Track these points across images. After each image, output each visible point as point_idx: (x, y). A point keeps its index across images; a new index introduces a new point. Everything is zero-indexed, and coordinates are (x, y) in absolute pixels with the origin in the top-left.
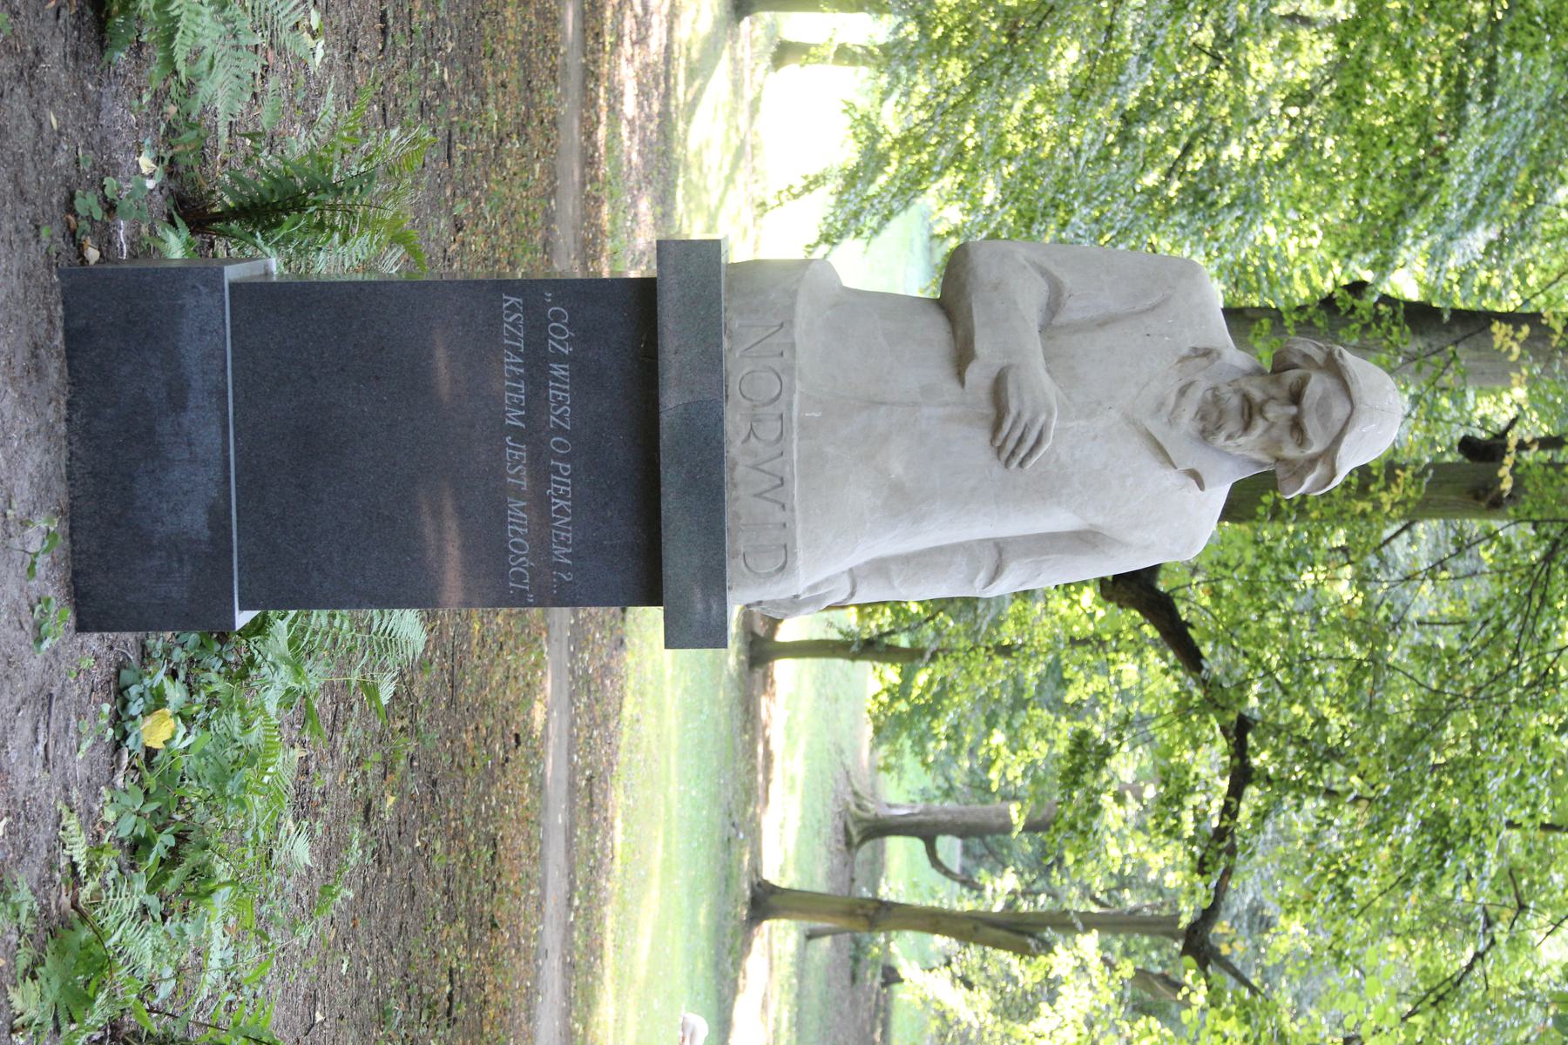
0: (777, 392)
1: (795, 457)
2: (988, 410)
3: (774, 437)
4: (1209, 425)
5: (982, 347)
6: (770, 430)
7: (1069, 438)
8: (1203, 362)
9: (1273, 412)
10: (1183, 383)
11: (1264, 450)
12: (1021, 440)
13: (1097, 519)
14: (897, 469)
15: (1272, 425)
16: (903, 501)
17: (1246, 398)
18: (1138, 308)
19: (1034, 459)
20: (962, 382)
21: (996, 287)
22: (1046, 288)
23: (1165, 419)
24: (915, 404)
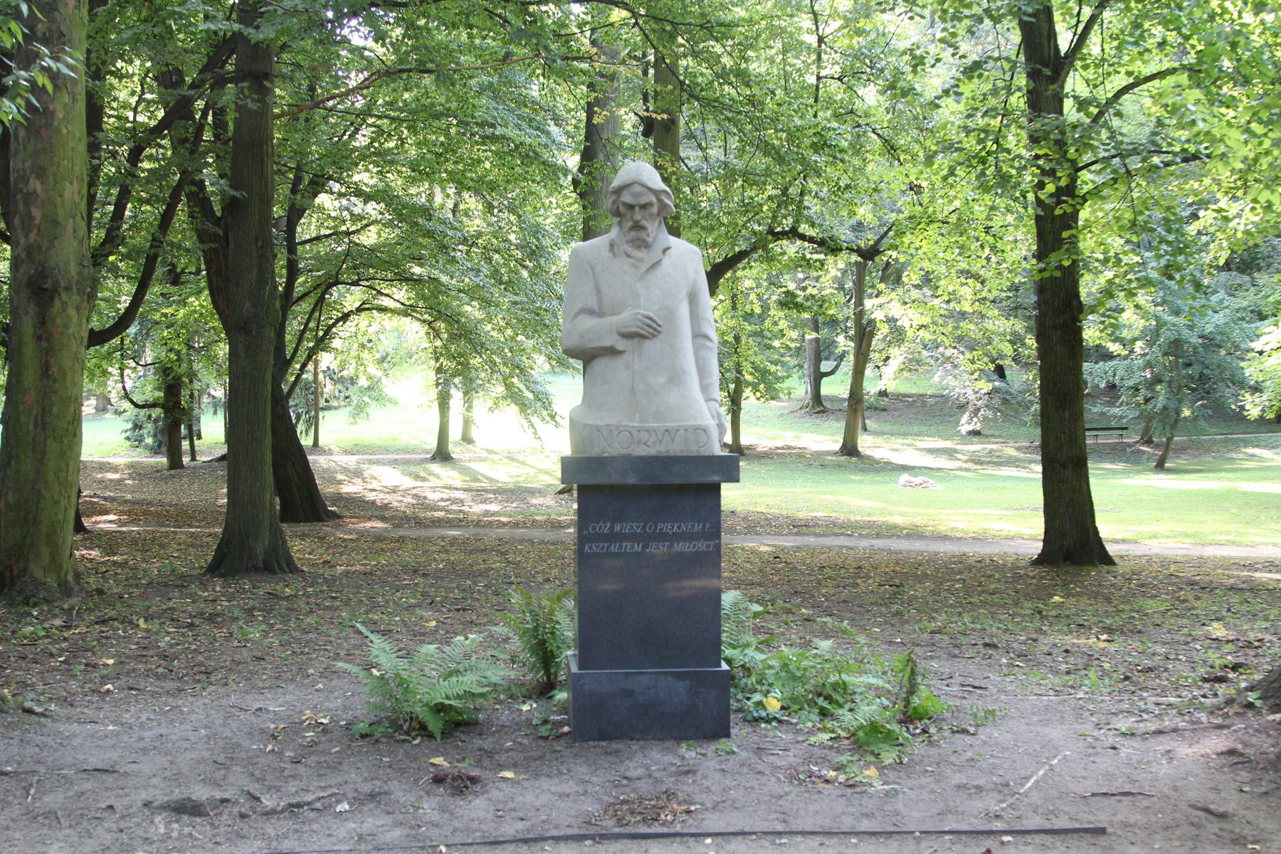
2: (636, 340)
4: (643, 245)
7: (649, 305)
9: (638, 217)
13: (684, 293)
14: (662, 380)
16: (676, 378)
17: (631, 228)
21: (582, 337)
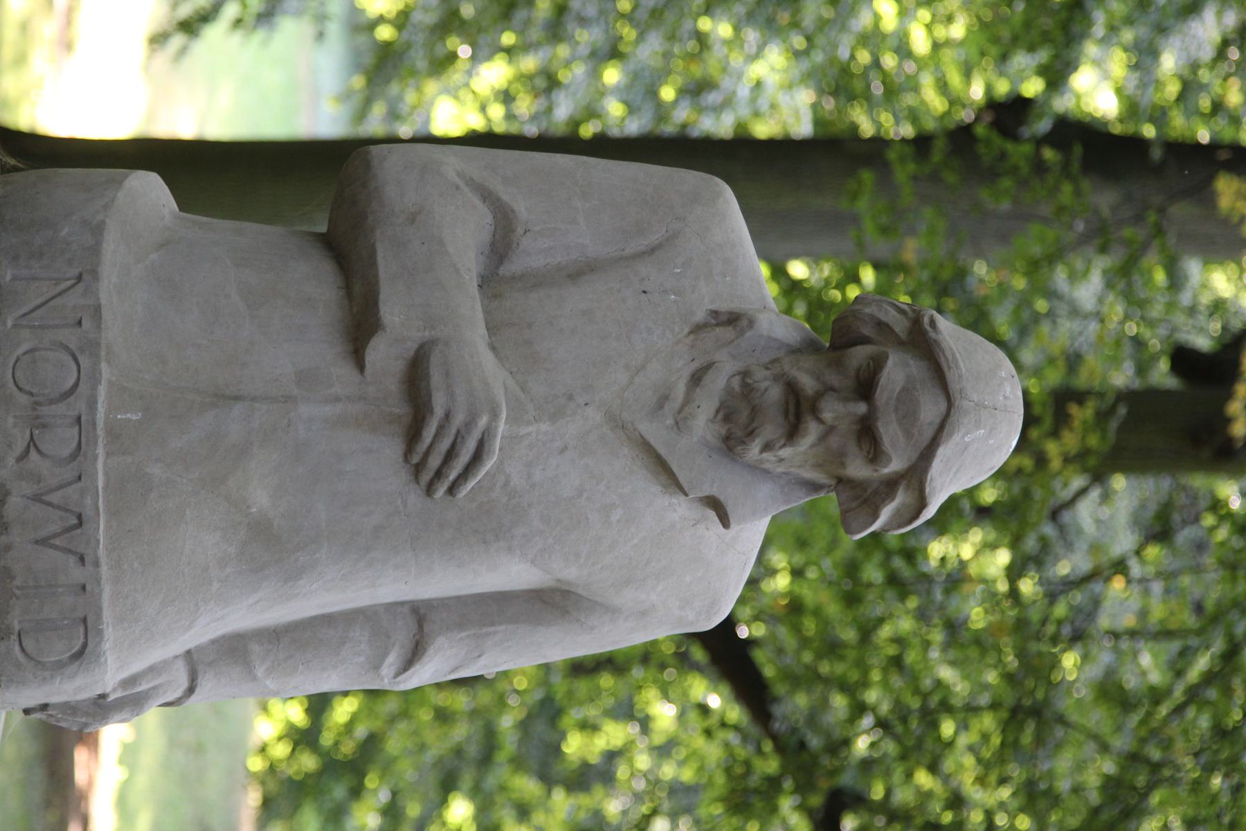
0: (71, 382)
1: (101, 485)
2: (401, 409)
3: (66, 452)
5: (392, 311)
6: (61, 441)
7: (523, 450)
8: (726, 333)
9: (832, 410)
10: (695, 366)
11: (818, 466)
12: (450, 455)
13: (570, 573)
15: (830, 430)
17: (792, 389)
18: (628, 251)
19: (471, 484)
20: (360, 365)
21: (412, 219)
22: (489, 219)
23: (670, 421)
24: (288, 399)
